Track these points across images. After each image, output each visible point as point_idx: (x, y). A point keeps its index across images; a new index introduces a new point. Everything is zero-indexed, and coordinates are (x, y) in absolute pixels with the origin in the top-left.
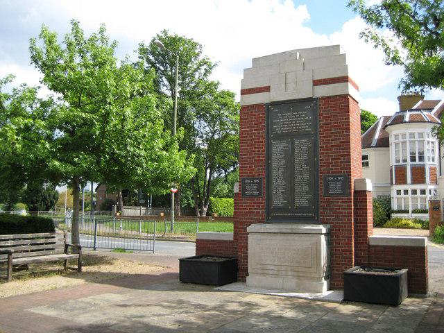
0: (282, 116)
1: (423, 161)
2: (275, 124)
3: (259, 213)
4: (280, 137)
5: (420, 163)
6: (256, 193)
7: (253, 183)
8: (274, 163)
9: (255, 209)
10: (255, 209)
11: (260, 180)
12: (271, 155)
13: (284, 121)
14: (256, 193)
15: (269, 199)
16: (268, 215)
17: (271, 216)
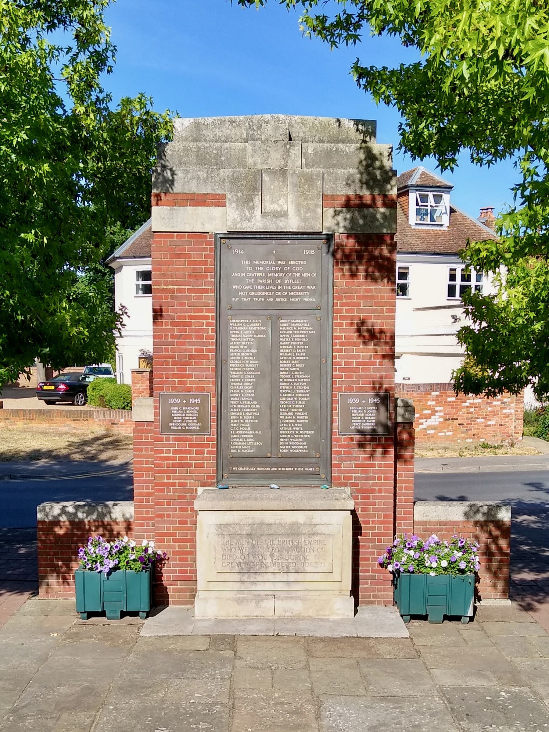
0: (252, 265)
1: (455, 281)
2: (240, 281)
3: (202, 465)
4: (242, 310)
5: (397, 274)
6: (195, 426)
7: (187, 405)
8: (234, 365)
9: (191, 459)
10: (191, 459)
11: (204, 398)
12: (227, 347)
13: (256, 278)
14: (195, 426)
15: (222, 435)
16: (220, 467)
17: (228, 470)
